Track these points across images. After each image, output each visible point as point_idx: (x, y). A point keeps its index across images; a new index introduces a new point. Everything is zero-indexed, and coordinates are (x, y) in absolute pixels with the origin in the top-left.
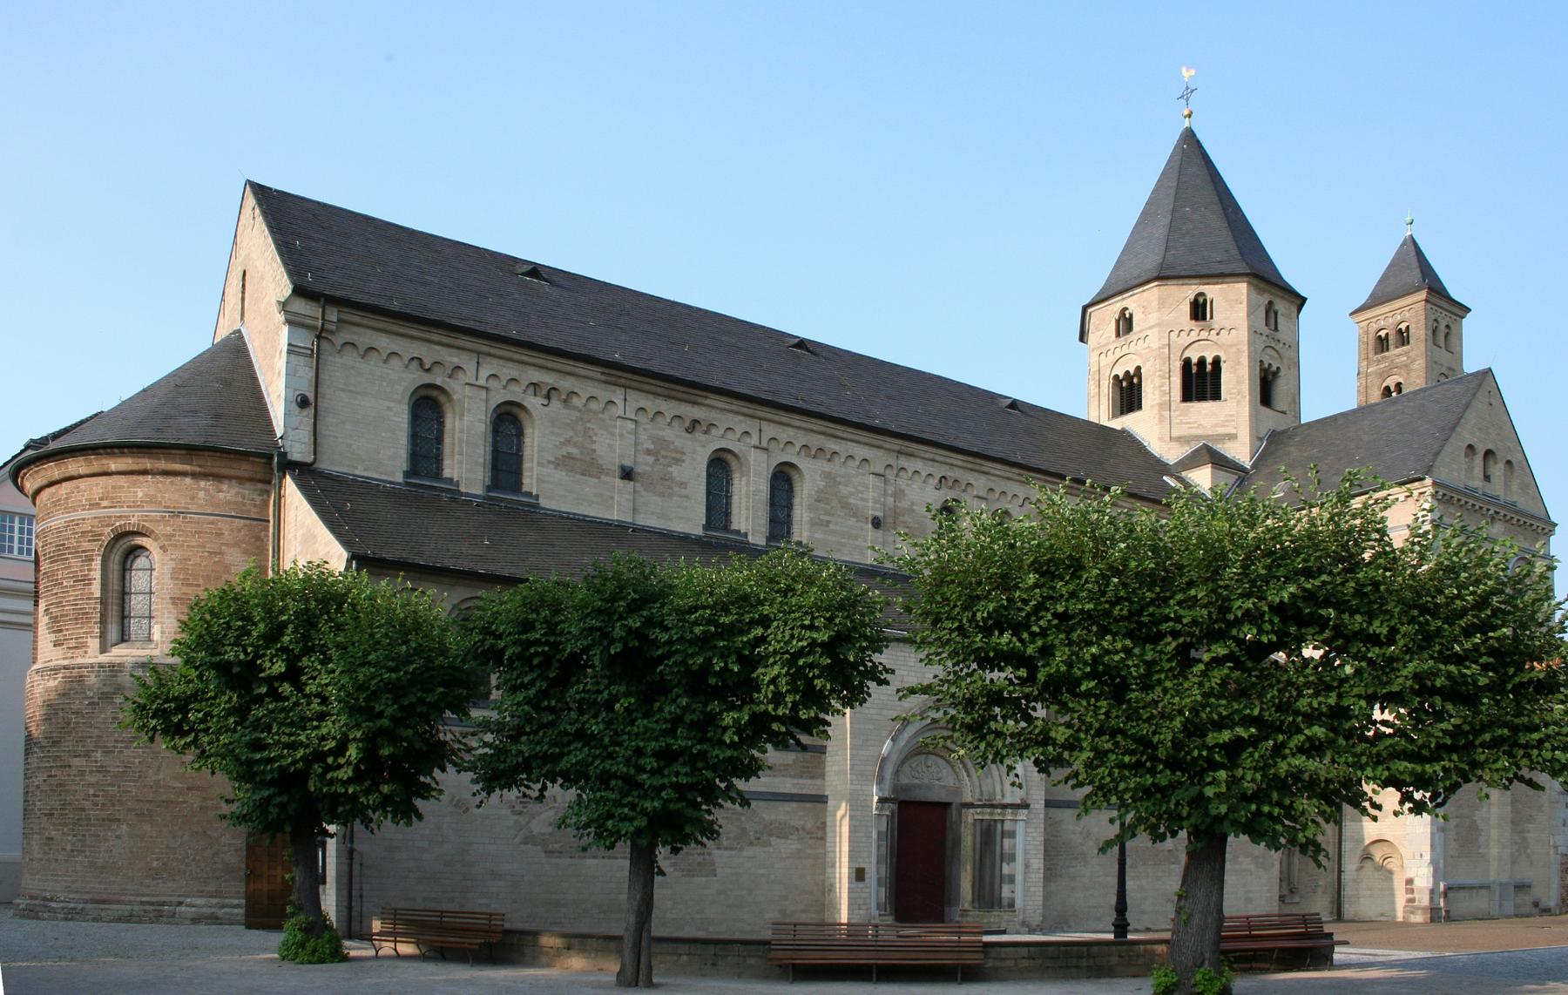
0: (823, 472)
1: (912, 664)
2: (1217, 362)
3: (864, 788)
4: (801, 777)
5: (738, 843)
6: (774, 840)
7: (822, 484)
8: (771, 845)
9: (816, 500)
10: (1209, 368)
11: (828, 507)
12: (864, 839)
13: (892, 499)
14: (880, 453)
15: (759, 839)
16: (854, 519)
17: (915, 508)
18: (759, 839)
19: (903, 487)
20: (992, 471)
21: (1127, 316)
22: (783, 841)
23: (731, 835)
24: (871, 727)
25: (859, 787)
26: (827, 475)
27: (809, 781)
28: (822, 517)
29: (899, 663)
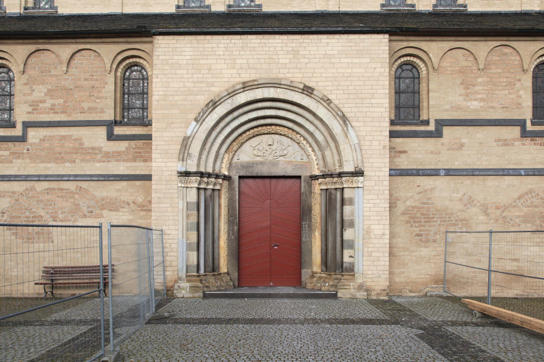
1: (221, 53)
3: (168, 164)
4: (135, 161)
5: (72, 216)
6: (105, 212)
8: (103, 217)
12: (169, 210)
15: (92, 212)
18: (92, 212)
22: (114, 213)
23: (66, 210)
24: (178, 111)
25: (164, 164)
27: (142, 164)
29: (206, 53)
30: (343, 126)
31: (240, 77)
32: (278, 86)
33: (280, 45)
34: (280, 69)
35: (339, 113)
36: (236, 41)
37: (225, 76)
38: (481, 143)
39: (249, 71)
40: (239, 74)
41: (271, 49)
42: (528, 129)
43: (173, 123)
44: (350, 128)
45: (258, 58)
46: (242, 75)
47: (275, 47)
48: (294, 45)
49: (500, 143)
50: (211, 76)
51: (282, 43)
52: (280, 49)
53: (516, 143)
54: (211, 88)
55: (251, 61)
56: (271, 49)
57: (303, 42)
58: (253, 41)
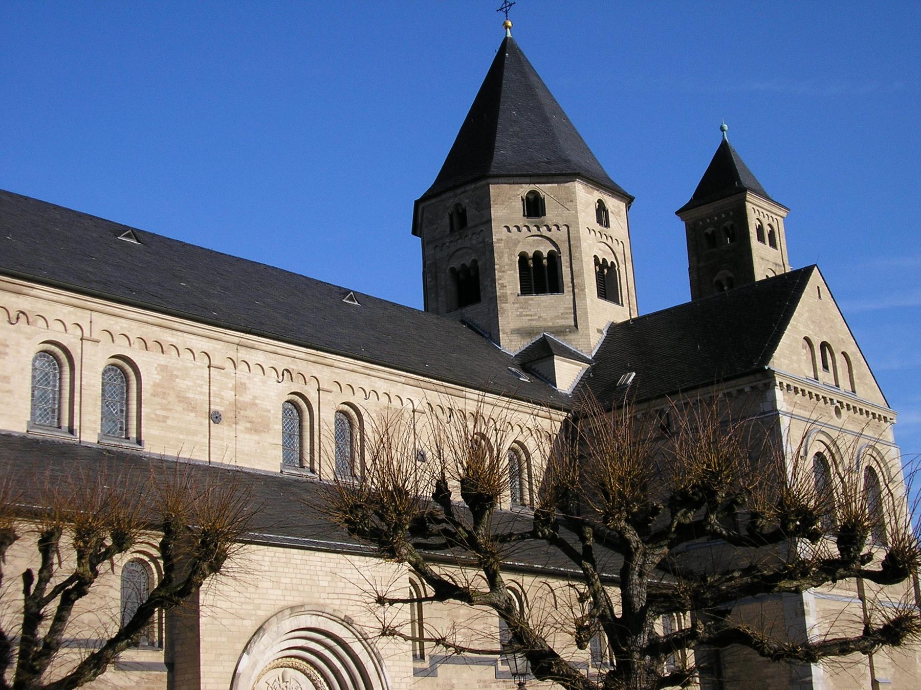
0: (159, 365)
2: (554, 258)
7: (157, 378)
9: (151, 395)
10: (545, 261)
11: (165, 402)
13: (233, 393)
14: (219, 345)
16: (193, 415)
17: (257, 401)
19: (243, 381)
20: (336, 364)
21: (460, 211)
26: (163, 368)
28: (158, 412)
30: (378, 665)
31: (285, 600)
32: (321, 614)
33: (319, 564)
34: (320, 593)
35: (375, 649)
36: (280, 555)
37: (271, 597)
38: (466, 685)
39: (293, 593)
40: (284, 596)
41: (312, 568)
42: (499, 669)
43: (221, 655)
44: (384, 668)
45: (300, 578)
46: (286, 598)
47: (315, 566)
48: (332, 565)
49: (481, 684)
50: (257, 596)
51: (321, 561)
52: (319, 568)
53: (493, 685)
54: (257, 611)
55: (294, 581)
56: (312, 568)
57: (339, 563)
58: (295, 556)
